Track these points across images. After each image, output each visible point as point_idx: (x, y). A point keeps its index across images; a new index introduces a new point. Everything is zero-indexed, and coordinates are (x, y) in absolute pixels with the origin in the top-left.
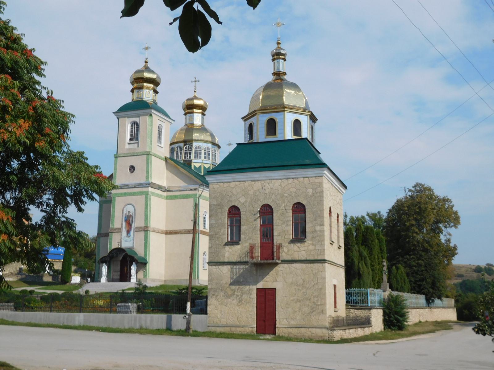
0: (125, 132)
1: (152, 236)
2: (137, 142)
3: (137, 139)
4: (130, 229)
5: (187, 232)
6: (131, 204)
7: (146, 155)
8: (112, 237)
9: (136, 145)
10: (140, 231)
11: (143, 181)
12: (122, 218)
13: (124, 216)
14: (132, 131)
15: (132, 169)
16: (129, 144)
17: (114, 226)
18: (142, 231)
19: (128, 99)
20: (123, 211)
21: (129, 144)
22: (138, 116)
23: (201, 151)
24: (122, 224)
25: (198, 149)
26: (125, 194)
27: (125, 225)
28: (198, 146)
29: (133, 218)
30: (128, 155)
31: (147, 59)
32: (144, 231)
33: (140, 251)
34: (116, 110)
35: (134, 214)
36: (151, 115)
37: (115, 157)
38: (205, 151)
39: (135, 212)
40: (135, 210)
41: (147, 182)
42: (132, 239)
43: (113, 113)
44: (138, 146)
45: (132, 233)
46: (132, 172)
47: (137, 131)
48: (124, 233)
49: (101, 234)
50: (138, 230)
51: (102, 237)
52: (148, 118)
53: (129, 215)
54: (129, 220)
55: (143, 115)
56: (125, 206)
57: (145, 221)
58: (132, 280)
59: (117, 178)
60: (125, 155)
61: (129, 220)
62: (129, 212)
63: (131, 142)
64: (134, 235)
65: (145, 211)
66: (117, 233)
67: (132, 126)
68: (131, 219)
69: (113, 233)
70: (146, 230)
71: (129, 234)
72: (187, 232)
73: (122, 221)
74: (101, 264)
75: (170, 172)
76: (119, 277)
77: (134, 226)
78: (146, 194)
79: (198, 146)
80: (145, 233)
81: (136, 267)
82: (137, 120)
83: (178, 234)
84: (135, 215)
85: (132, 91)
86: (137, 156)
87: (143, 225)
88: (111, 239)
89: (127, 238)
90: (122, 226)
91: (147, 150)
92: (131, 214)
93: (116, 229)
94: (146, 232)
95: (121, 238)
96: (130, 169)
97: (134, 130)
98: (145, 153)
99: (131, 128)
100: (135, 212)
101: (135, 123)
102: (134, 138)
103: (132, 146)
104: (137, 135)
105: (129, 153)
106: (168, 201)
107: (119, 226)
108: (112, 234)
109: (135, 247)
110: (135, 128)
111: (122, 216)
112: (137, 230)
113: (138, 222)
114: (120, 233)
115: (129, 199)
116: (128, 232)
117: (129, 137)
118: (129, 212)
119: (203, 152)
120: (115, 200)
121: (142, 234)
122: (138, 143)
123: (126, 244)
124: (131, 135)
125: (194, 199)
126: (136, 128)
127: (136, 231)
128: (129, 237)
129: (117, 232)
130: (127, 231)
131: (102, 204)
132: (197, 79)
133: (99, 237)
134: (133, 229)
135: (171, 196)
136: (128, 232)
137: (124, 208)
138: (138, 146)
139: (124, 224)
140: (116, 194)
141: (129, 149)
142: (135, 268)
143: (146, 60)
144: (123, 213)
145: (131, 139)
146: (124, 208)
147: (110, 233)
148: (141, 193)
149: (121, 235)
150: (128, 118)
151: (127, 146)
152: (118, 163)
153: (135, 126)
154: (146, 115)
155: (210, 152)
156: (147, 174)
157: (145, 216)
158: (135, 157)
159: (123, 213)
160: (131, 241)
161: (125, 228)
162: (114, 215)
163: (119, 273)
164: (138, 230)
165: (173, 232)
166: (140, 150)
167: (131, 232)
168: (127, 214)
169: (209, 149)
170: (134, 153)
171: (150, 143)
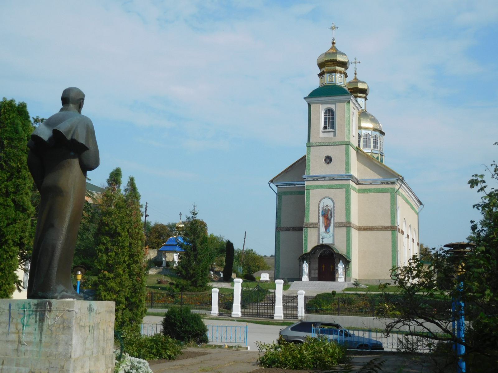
0: (318, 119)
1: (354, 233)
2: (333, 130)
3: (332, 128)
4: (329, 224)
5: (385, 228)
6: (329, 198)
7: (345, 145)
8: (307, 232)
9: (332, 133)
10: (341, 227)
11: (343, 172)
12: (319, 213)
13: (321, 210)
14: (325, 119)
15: (328, 159)
16: (322, 132)
18: (343, 227)
19: (315, 83)
20: (319, 204)
21: (323, 132)
22: (334, 103)
23: (370, 139)
24: (319, 219)
25: (367, 137)
26: (321, 187)
27: (323, 219)
28: (367, 135)
29: (331, 213)
30: (324, 145)
31: (333, 40)
32: (346, 227)
33: (341, 248)
34: (307, 95)
35: (332, 208)
36: (349, 102)
37: (307, 146)
38: (374, 139)
39: (334, 207)
40: (334, 203)
41: (348, 174)
42: (331, 235)
43: (305, 98)
44: (335, 135)
45: (331, 228)
46: (328, 163)
47: (333, 118)
48: (322, 228)
49: (280, 228)
50: (339, 225)
52: (345, 104)
53: (327, 209)
54: (328, 215)
55: (340, 102)
57: (346, 216)
58: (340, 280)
59: (311, 169)
60: (320, 145)
61: (327, 215)
63: (326, 130)
64: (334, 230)
65: (346, 206)
66: (313, 228)
67: (326, 112)
68: (329, 213)
69: (309, 228)
70: (348, 226)
71: (328, 230)
72: (385, 228)
73: (319, 216)
74: (301, 262)
75: (362, 163)
76: (316, 276)
78: (347, 188)
79: (367, 135)
80: (346, 229)
81: (344, 266)
82: (332, 106)
83: (374, 230)
84: (334, 209)
85: (321, 75)
86: (334, 146)
87: (344, 220)
88: (307, 234)
89: (325, 234)
90: (319, 221)
91: (346, 140)
93: (312, 224)
94: (349, 228)
95: (318, 234)
96: (325, 160)
97: (329, 117)
98: (344, 144)
99: (325, 115)
100: (334, 207)
101: (329, 110)
102: (329, 126)
103: (326, 135)
104: (332, 123)
105: (324, 143)
106: (361, 194)
107: (316, 221)
108: (308, 230)
109: (335, 244)
110: (329, 115)
112: (338, 226)
113: (338, 217)
114: (317, 229)
115: (326, 192)
116: (327, 227)
117: (322, 125)
118: (327, 206)
119: (372, 140)
120: (309, 193)
121: (344, 230)
122: (335, 132)
123: (327, 241)
124: (325, 123)
125: (391, 194)
126: (331, 115)
128: (328, 233)
129: (314, 227)
130: (325, 227)
131: (281, 196)
132: (357, 61)
133: (278, 231)
134: (332, 225)
135: (364, 189)
136: (327, 227)
137: (320, 201)
138: (335, 135)
139: (321, 218)
140: (311, 186)
141: (325, 138)
142: (342, 266)
143: (333, 41)
144: (319, 207)
145: (325, 128)
146: (320, 201)
147: (305, 227)
148: (341, 187)
149: (318, 231)
150: (321, 104)
151: (321, 135)
152: (311, 153)
153: (329, 113)
154: (344, 102)
155: (377, 140)
156: (346, 165)
157: (346, 211)
158: (332, 147)
159: (319, 207)
160: (330, 237)
162: (309, 209)
163: (317, 271)
164: (339, 225)
165: (368, 228)
166: (338, 139)
167: (330, 227)
169: (377, 138)
170: (330, 142)
171: (348, 131)
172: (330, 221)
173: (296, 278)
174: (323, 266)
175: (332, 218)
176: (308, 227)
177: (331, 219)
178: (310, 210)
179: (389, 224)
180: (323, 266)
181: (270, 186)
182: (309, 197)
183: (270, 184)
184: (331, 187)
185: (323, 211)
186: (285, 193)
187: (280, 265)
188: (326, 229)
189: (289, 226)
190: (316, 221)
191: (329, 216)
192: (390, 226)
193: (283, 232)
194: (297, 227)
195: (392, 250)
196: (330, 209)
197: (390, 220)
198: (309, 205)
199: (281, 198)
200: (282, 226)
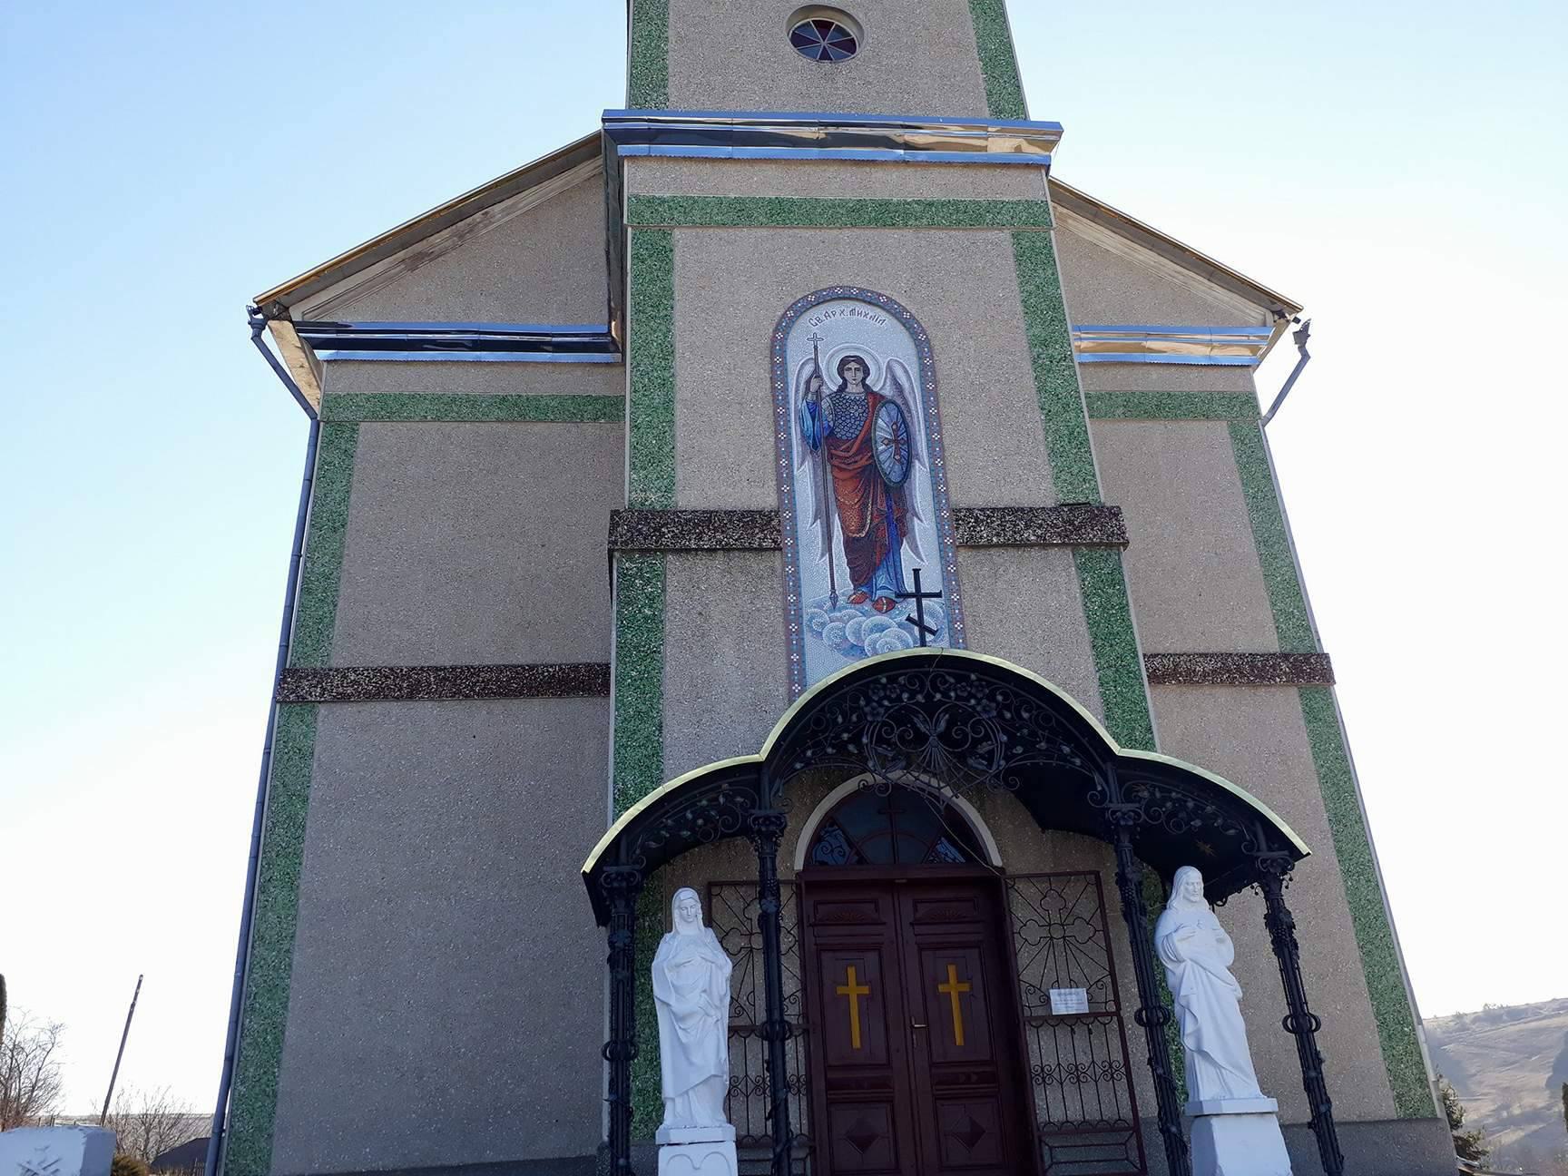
4: (896, 523)
13: (796, 401)
17: (669, 489)
20: (777, 349)
24: (784, 479)
27: (820, 487)
39: (928, 372)
40: (923, 346)
49: (321, 676)
51: (343, 698)
54: (867, 443)
56: (800, 308)
62: (853, 364)
71: (881, 579)
73: (783, 450)
77: (937, 495)
90: (787, 496)
92: (877, 382)
93: (707, 520)
95: (793, 614)
108: (661, 577)
111: (778, 397)
120: (664, 254)
127: (972, 545)
130: (850, 544)
133: (302, 700)
134: (924, 527)
137: (784, 326)
139: (805, 476)
144: (778, 370)
146: (784, 326)
161: (823, 515)
162: (666, 385)
167: (905, 547)
168: (832, 384)
172: (896, 495)
173: (455, 1162)
174: (854, 990)
175: (920, 474)
176: (665, 551)
177: (906, 474)
178: (683, 392)
179: (1274, 646)
180: (854, 990)
181: (257, 338)
182: (668, 292)
183: (258, 328)
184: (886, 215)
185: (814, 409)
186: (388, 408)
187: (291, 1032)
188: (862, 576)
189: (404, 661)
190: (765, 498)
191: (884, 453)
192: (1285, 656)
193: (348, 710)
194: (490, 669)
195: (1339, 851)
196: (888, 392)
197: (1266, 614)
198: (668, 353)
199: (352, 439)
200: (337, 662)
